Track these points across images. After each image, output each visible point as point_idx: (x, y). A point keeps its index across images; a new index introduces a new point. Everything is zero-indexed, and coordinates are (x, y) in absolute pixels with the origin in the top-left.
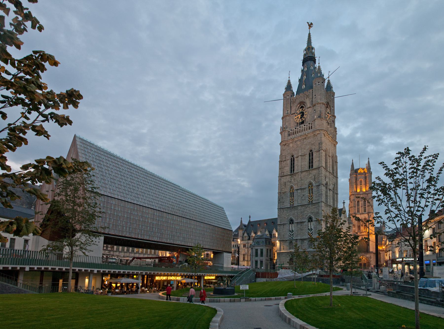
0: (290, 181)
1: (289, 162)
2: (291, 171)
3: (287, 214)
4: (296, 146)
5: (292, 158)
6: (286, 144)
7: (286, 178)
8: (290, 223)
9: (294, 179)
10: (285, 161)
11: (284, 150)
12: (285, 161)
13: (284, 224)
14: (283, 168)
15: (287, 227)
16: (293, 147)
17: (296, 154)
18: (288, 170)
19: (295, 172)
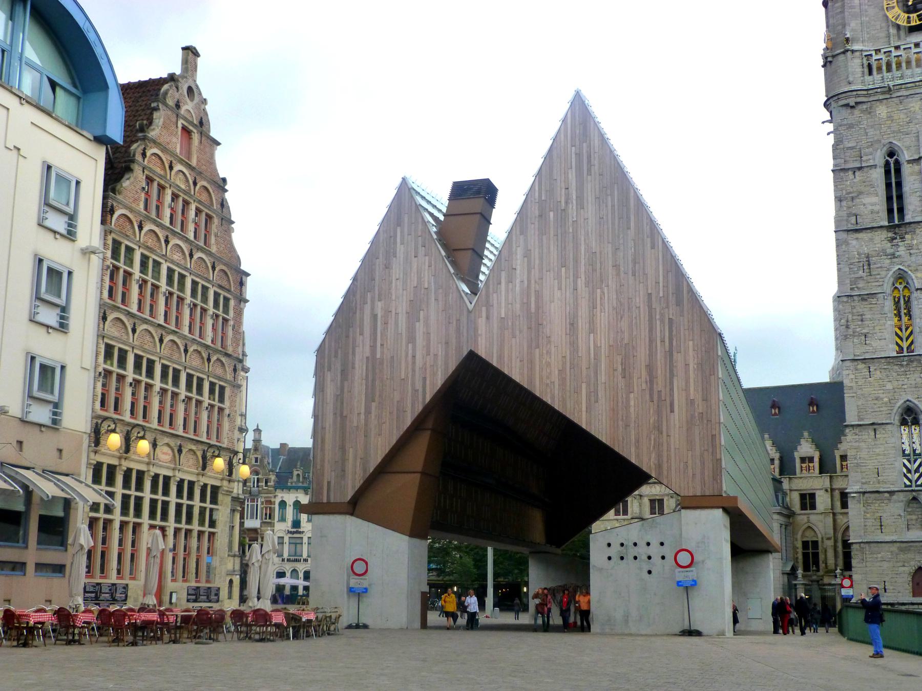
0: (889, 251)
1: (878, 176)
2: (890, 211)
3: (889, 386)
4: (902, 116)
5: (892, 161)
6: (857, 103)
7: (871, 240)
8: (904, 422)
9: (910, 247)
10: (860, 168)
11: (850, 126)
12: (860, 168)
13: (874, 426)
14: (853, 199)
15: (893, 440)
16: (890, 117)
17: (908, 148)
18: (876, 208)
19: (908, 218)
